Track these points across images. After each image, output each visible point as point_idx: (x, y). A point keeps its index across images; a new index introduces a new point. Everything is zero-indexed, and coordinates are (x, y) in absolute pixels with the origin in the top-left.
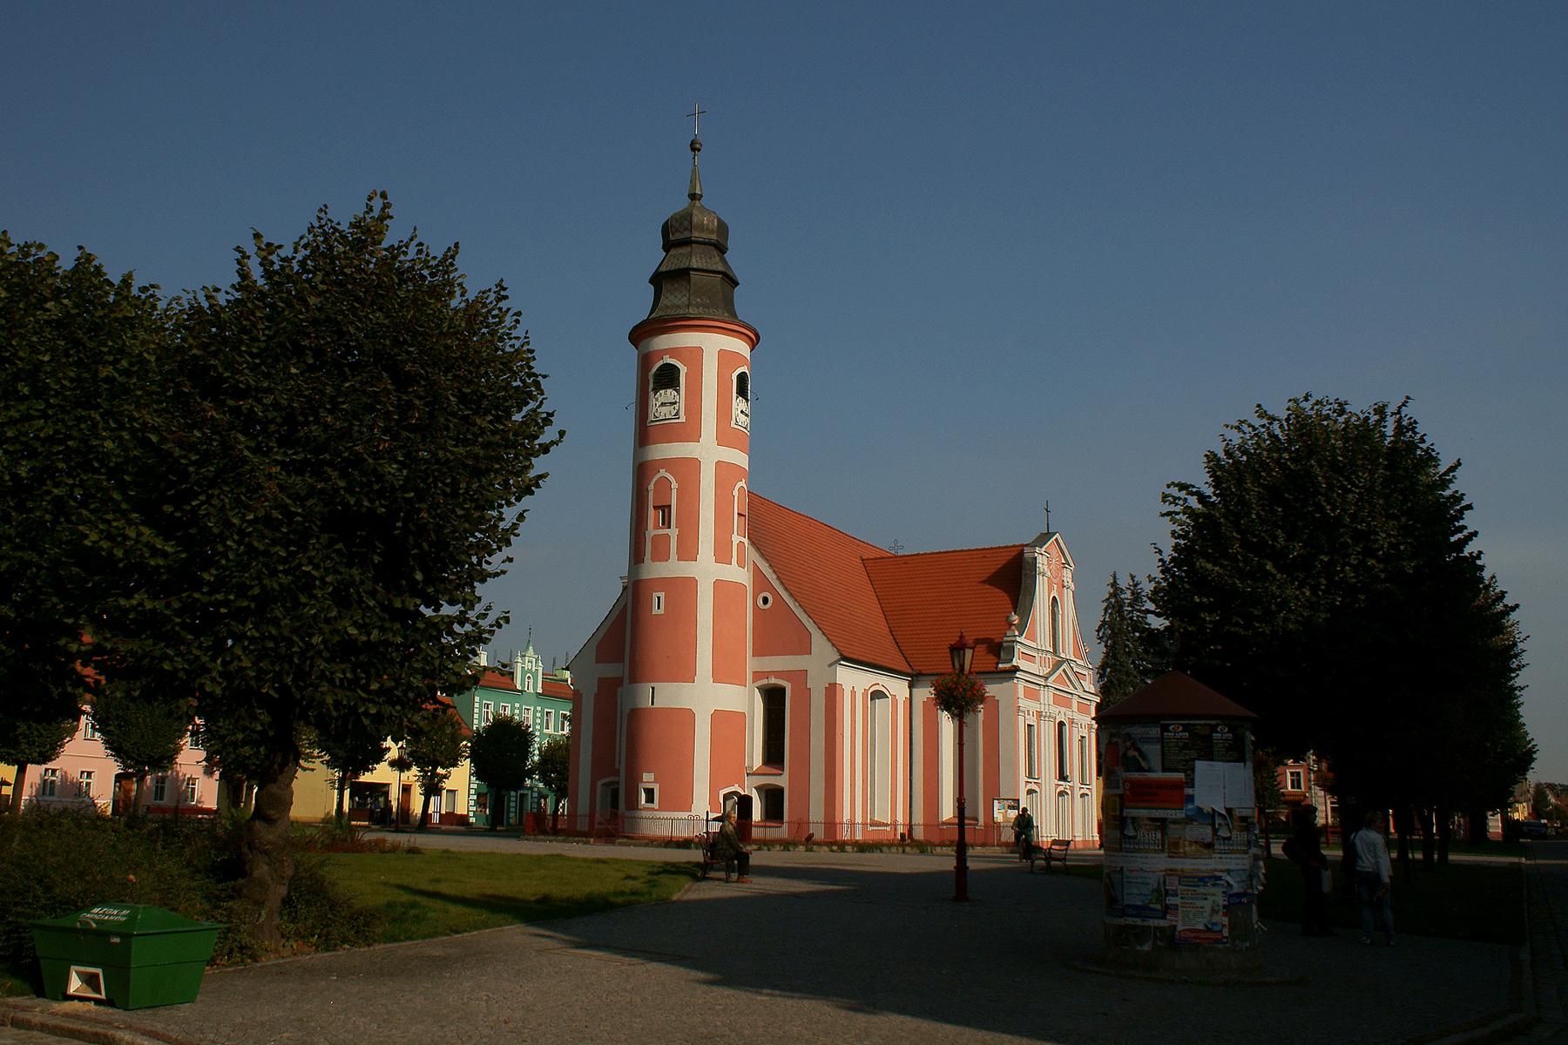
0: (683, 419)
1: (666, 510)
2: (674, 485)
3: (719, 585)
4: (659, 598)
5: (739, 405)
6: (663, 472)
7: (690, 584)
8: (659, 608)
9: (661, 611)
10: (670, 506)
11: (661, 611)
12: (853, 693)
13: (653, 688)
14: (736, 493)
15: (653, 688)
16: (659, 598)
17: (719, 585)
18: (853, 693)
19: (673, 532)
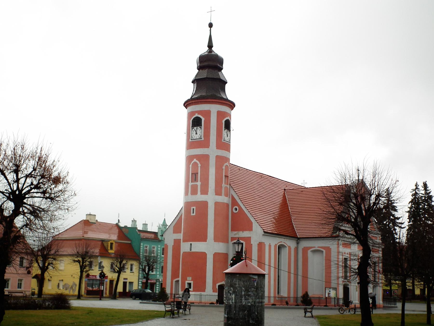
0: (203, 139)
1: (197, 175)
2: (199, 165)
3: (216, 204)
4: (193, 209)
5: (225, 132)
6: (195, 160)
7: (205, 204)
8: (193, 213)
9: (194, 214)
10: (198, 173)
11: (194, 214)
12: (270, 246)
13: (191, 244)
14: (224, 167)
15: (191, 244)
16: (193, 209)
17: (216, 204)
18: (270, 246)
19: (199, 183)
